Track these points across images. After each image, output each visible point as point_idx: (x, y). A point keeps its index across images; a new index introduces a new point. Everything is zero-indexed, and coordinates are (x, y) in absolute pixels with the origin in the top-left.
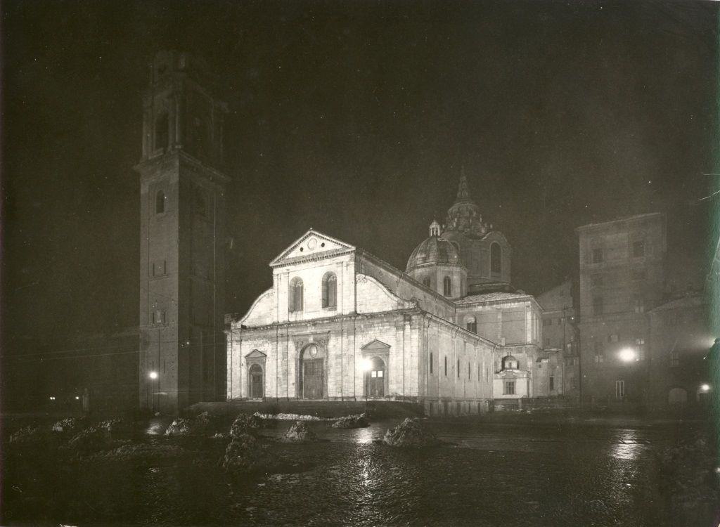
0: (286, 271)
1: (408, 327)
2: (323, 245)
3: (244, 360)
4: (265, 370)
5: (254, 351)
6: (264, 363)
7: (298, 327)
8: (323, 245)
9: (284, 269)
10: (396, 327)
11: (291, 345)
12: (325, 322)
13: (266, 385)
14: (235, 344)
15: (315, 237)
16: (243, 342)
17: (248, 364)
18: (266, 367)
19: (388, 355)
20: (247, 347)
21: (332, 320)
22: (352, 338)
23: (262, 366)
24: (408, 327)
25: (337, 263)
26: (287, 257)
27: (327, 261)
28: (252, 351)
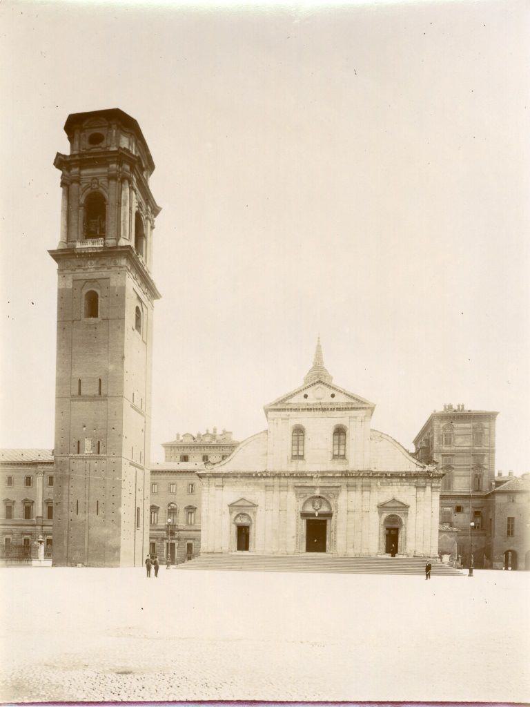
0: (285, 417)
1: (428, 489)
2: (333, 396)
3: (227, 509)
4: (255, 521)
5: (242, 499)
6: (255, 513)
7: (301, 477)
8: (333, 396)
9: (283, 414)
10: (417, 487)
11: (291, 495)
12: (338, 475)
13: (257, 537)
14: (213, 488)
15: (322, 386)
16: (226, 488)
17: (231, 513)
18: (258, 516)
19: (406, 514)
20: (231, 493)
21: (346, 475)
22: (366, 494)
23: (251, 516)
24: (428, 489)
25: (350, 417)
26: (287, 402)
27: (339, 413)
28: (239, 499)
